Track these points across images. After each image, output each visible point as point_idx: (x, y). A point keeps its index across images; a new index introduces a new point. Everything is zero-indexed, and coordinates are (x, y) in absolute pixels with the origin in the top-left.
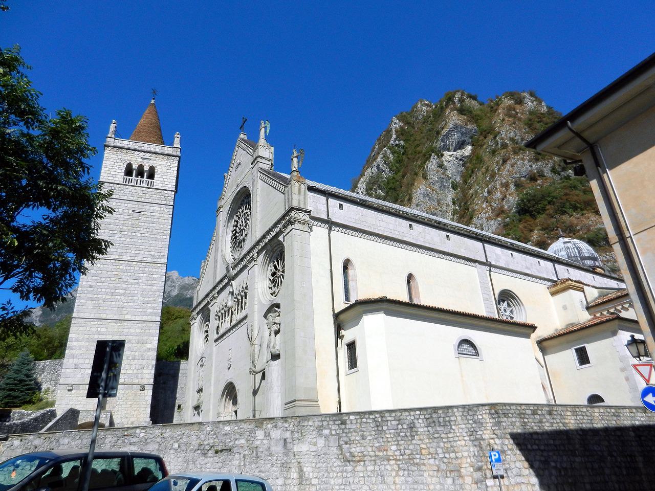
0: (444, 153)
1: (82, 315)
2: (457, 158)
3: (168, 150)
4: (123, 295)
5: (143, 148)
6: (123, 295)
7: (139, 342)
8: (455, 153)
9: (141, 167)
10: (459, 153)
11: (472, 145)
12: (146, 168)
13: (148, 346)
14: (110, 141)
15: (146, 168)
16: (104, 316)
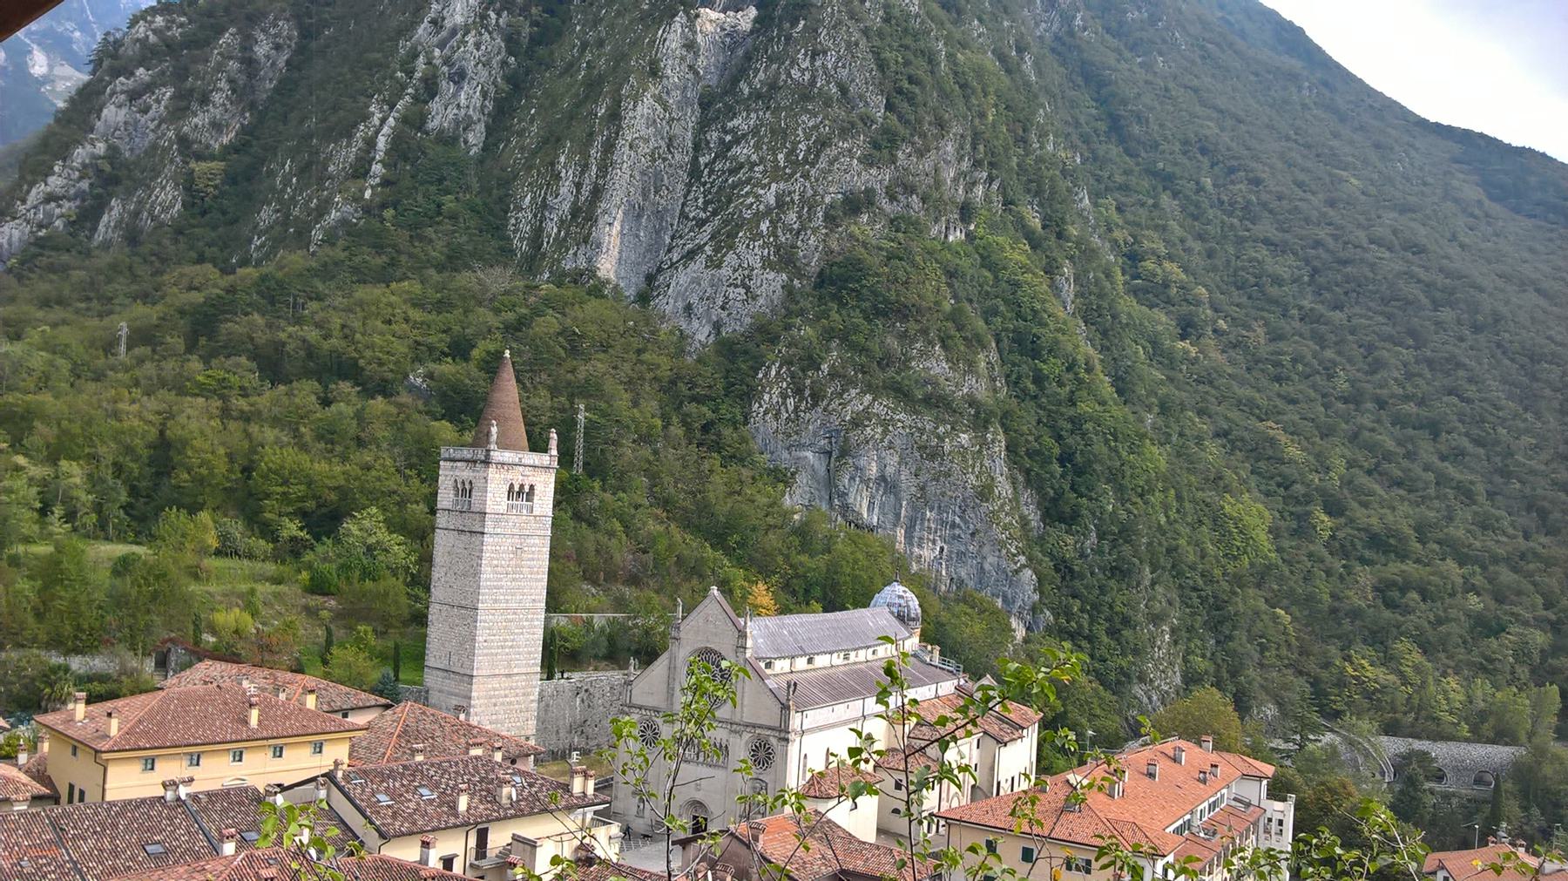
0: (702, 10)
1: (480, 673)
2: (723, 29)
3: (543, 459)
4: (511, 647)
5: (525, 461)
6: (511, 647)
7: (524, 694)
8: (722, 15)
9: (522, 486)
10: (730, 18)
11: (757, 9)
12: (527, 489)
13: (532, 698)
14: (497, 455)
15: (527, 489)
16: (497, 672)
